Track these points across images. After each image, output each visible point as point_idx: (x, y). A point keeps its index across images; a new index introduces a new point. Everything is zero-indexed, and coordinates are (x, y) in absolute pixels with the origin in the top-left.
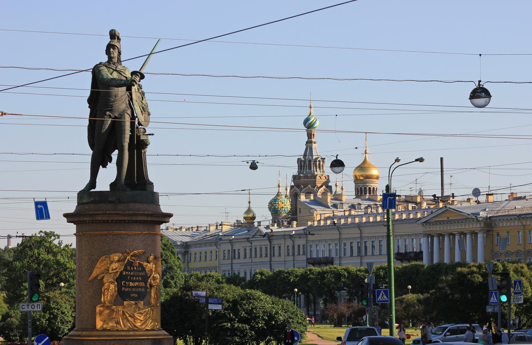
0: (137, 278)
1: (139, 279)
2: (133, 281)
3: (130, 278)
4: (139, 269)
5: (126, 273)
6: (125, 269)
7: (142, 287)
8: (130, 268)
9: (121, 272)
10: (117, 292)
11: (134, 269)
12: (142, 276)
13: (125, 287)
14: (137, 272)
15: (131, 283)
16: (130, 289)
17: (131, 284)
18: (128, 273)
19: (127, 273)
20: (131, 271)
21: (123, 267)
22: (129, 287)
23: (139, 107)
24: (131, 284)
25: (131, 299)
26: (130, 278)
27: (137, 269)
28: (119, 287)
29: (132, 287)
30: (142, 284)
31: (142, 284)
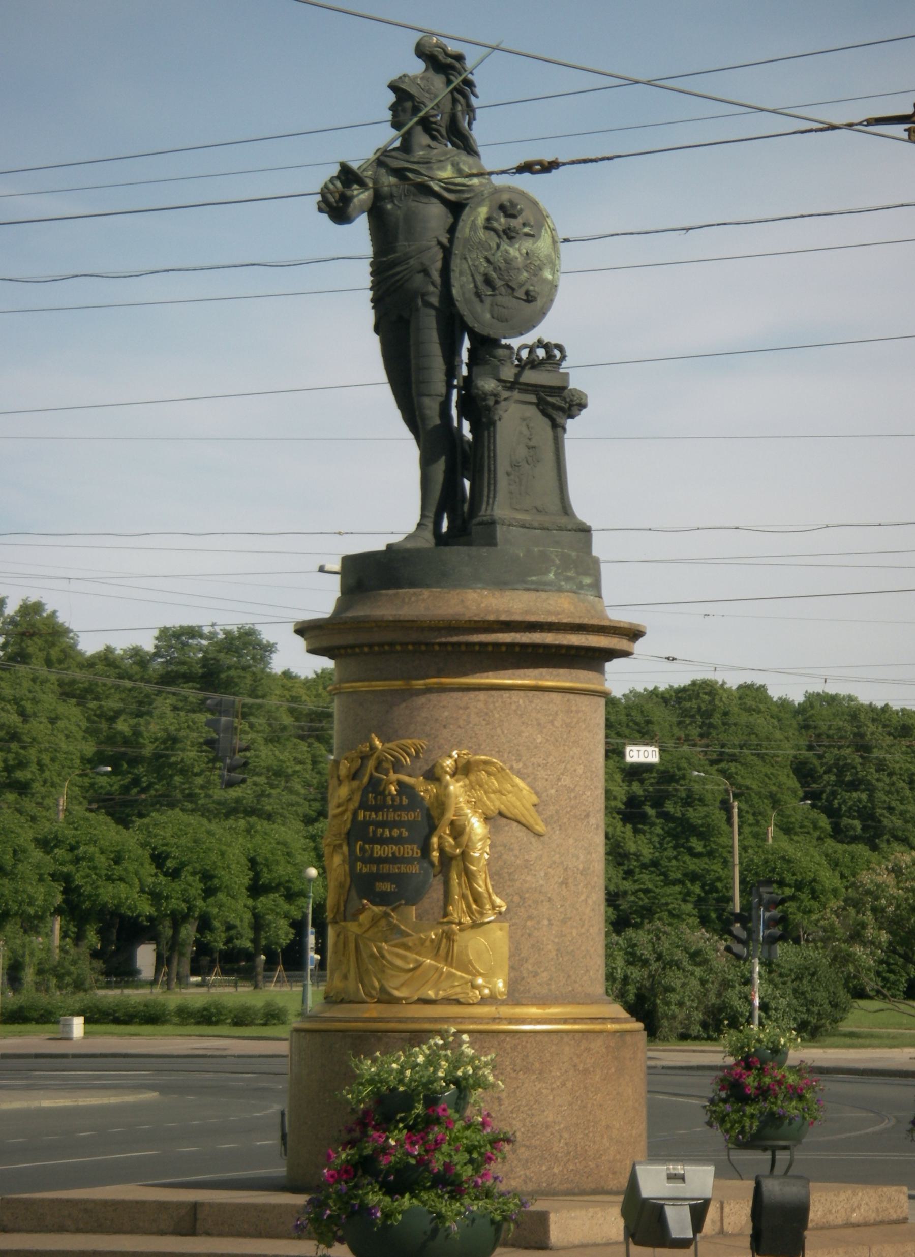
0: (396, 832)
1: (401, 833)
2: (382, 841)
3: (374, 832)
4: (401, 800)
5: (365, 817)
6: (363, 805)
7: (410, 861)
8: (375, 798)
9: (355, 814)
10: (348, 880)
11: (385, 800)
12: (410, 825)
13: (365, 861)
14: (395, 811)
15: (377, 847)
16: (374, 869)
17: (379, 851)
18: (370, 816)
19: (367, 813)
20: (377, 809)
21: (357, 798)
22: (372, 860)
23: (470, 279)
24: (379, 851)
25: (378, 900)
26: (374, 832)
27: (393, 800)
28: (352, 860)
29: (381, 861)
30: (412, 850)
31: (412, 850)
